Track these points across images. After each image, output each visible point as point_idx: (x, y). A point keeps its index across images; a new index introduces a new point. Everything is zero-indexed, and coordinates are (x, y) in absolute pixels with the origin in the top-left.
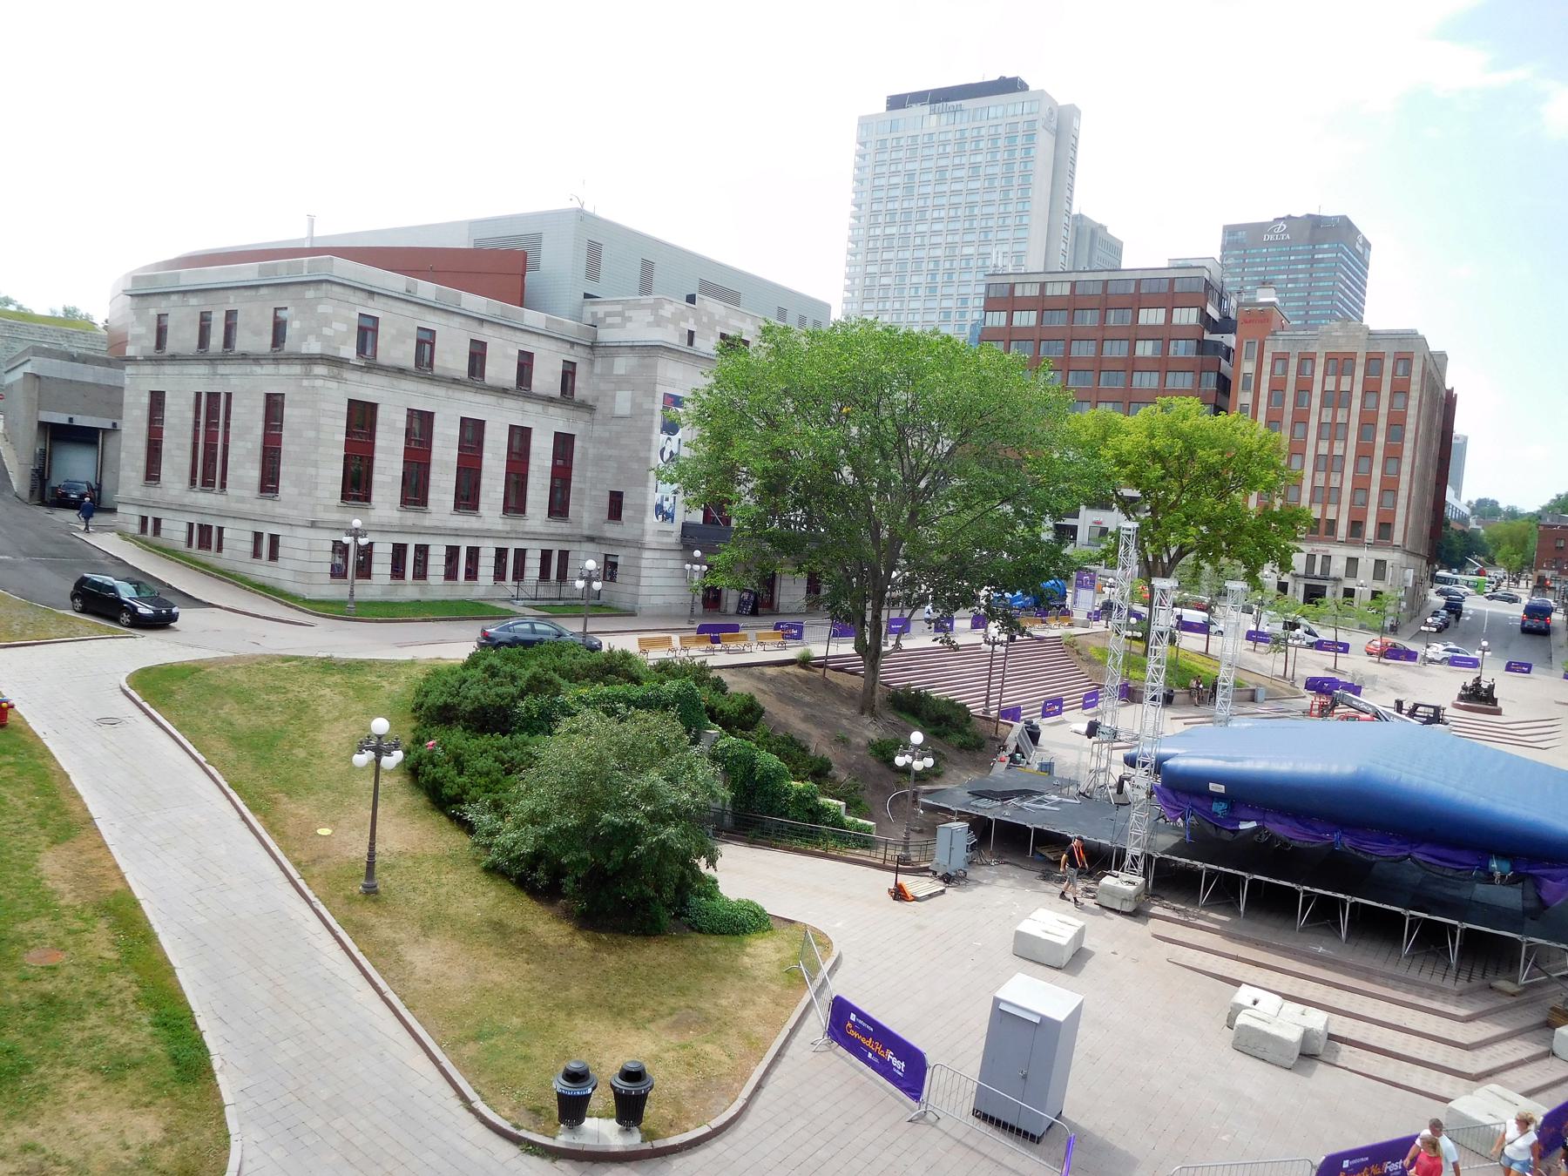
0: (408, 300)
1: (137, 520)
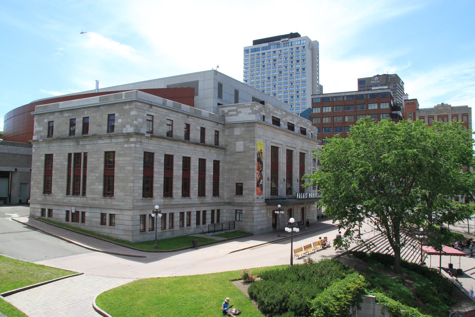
0: (163, 107)
1: (40, 210)
